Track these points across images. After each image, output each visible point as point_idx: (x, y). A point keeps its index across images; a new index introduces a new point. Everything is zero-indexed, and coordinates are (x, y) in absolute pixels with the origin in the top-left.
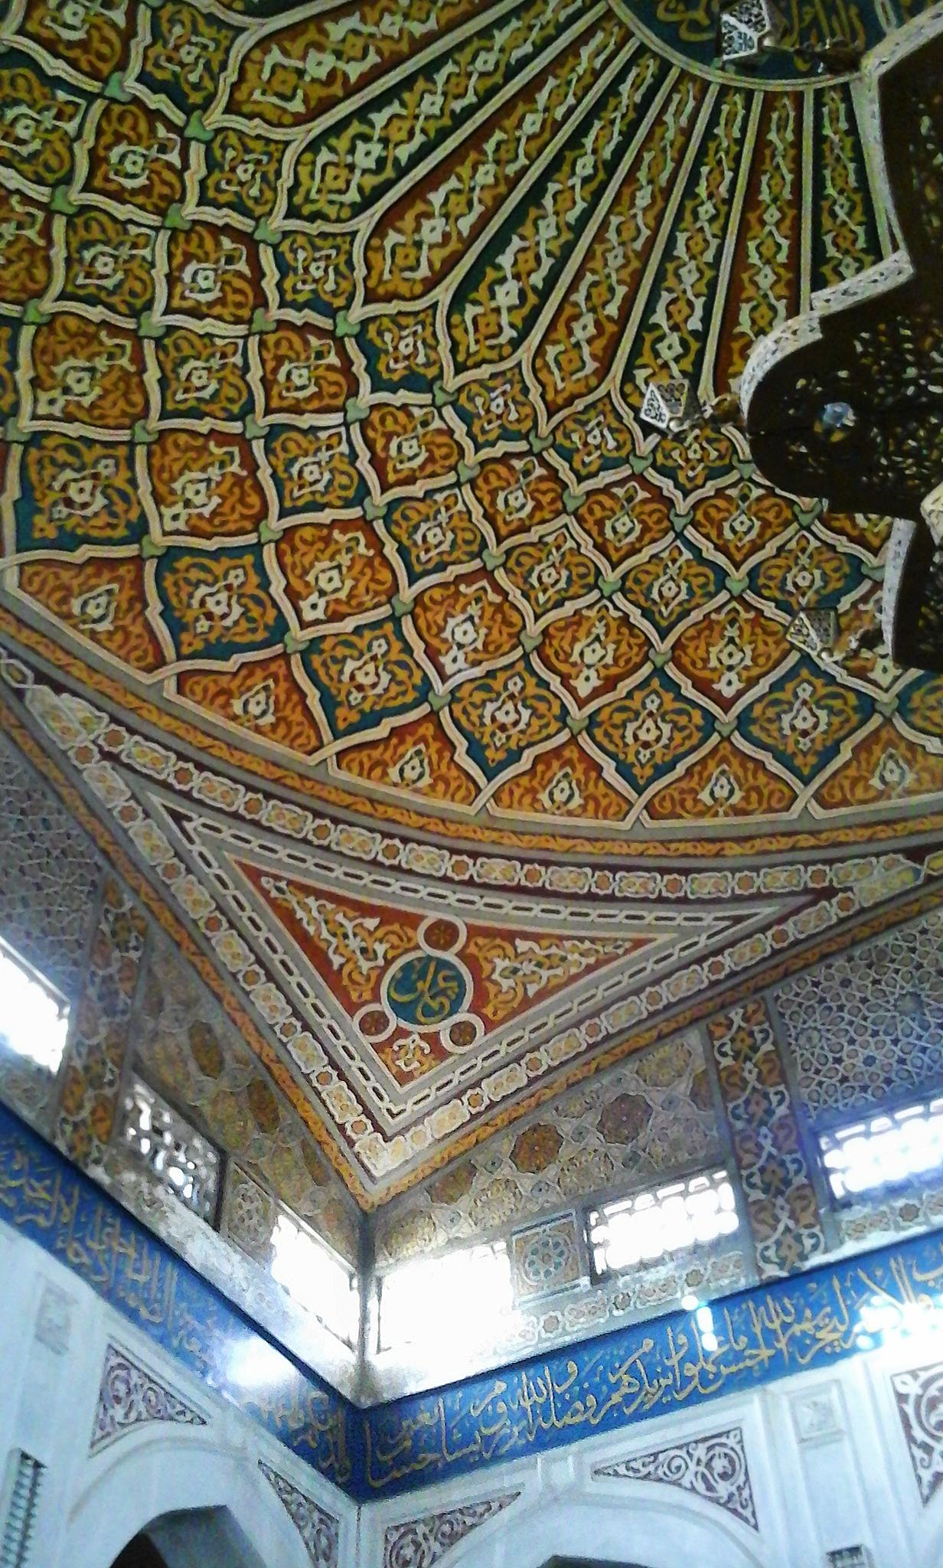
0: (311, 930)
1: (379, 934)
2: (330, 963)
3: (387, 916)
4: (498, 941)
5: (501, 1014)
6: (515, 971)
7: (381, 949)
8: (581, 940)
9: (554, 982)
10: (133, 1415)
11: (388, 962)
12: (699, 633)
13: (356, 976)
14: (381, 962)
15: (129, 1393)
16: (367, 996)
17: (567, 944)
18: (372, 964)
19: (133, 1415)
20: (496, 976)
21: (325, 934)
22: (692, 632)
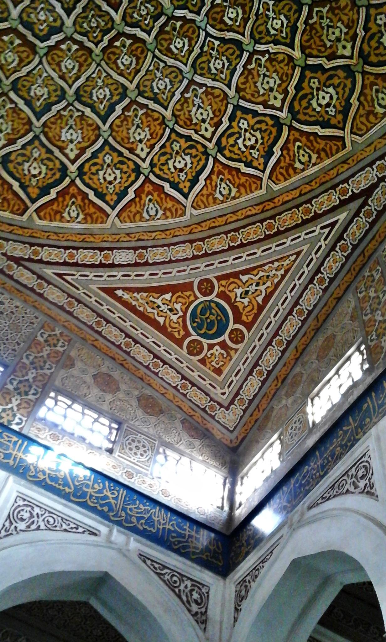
0: (141, 309)
1: (174, 299)
2: (159, 323)
3: (173, 289)
4: (232, 280)
5: (250, 318)
6: (247, 292)
7: (178, 306)
8: (272, 262)
9: (269, 290)
10: (34, 527)
11: (185, 313)
12: (246, 78)
13: (172, 325)
14: (181, 314)
15: (32, 516)
16: (182, 333)
17: (266, 267)
18: (177, 316)
19: (34, 527)
20: (238, 299)
21: (149, 310)
22: (242, 80)
